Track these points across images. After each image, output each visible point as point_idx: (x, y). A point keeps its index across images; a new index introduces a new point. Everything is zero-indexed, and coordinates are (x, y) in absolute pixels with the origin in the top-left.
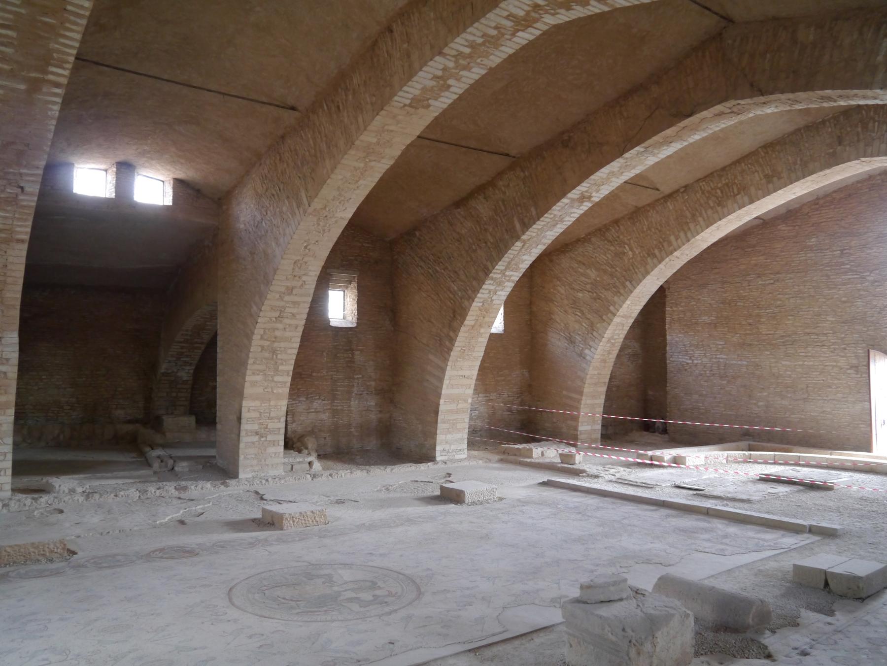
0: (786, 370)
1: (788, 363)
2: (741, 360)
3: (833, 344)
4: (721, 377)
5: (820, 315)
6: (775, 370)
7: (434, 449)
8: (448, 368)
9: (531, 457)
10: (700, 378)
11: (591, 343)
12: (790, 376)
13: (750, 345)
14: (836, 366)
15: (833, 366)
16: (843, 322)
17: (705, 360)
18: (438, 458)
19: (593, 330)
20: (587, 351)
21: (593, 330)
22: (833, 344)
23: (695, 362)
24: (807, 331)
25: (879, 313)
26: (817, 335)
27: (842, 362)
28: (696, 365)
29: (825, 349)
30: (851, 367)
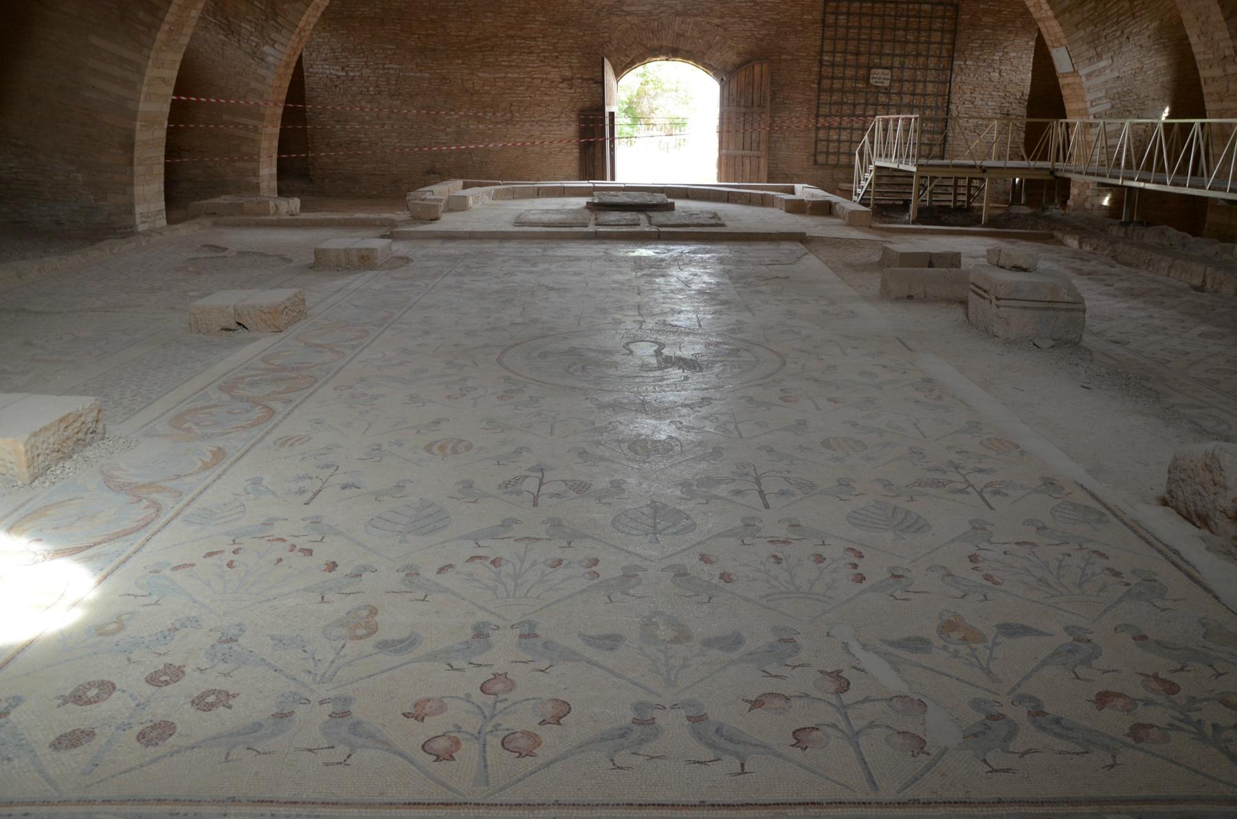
0: (483, 85)
1: (486, 75)
2: (421, 71)
3: (543, 51)
4: (392, 96)
5: (527, 13)
6: (469, 85)
7: (131, 212)
8: (150, 63)
9: (267, 213)
10: (360, 97)
11: (273, 35)
12: (488, 93)
13: (434, 50)
14: (546, 79)
15: (543, 80)
16: (555, 23)
17: (366, 71)
18: (141, 228)
19: (277, 14)
20: (267, 49)
21: (277, 14)
22: (543, 51)
23: (351, 74)
24: (512, 33)
25: (597, 14)
26: (523, 38)
27: (554, 75)
28: (353, 79)
29: (534, 57)
30: (564, 80)
